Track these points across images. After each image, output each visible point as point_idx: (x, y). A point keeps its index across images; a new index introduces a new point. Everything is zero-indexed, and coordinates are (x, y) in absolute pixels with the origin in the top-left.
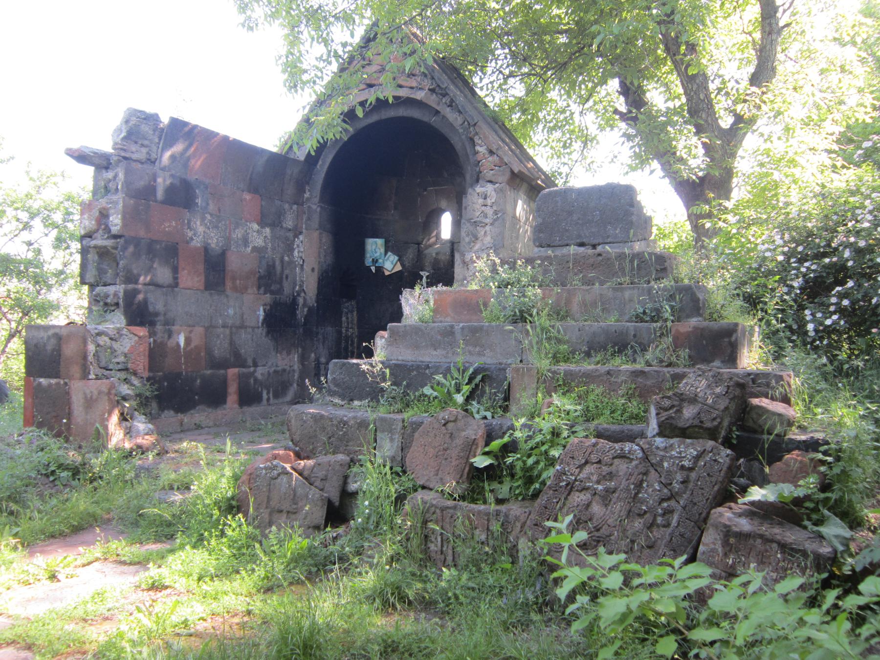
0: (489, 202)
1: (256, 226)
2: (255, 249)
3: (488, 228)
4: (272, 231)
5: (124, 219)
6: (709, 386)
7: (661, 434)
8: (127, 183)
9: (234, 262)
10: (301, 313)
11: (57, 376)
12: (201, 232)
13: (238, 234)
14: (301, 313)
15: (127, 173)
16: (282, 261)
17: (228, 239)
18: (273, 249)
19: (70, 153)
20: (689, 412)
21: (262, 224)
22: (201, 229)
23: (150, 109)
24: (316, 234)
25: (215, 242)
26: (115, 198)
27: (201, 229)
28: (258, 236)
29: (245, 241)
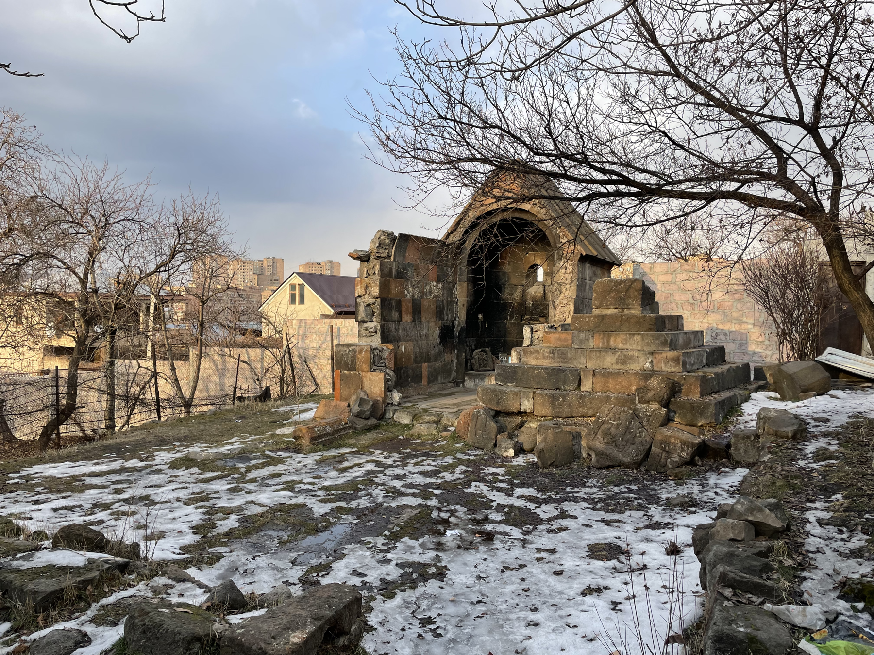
0: (568, 271)
1: (435, 283)
2: (435, 297)
3: (568, 286)
4: (443, 286)
5: (380, 289)
6: (658, 384)
7: (639, 402)
8: (381, 270)
9: (425, 303)
10: (457, 329)
11: (355, 369)
12: (411, 292)
13: (427, 289)
14: (457, 329)
15: (381, 265)
16: (447, 301)
17: (423, 292)
18: (443, 295)
19: (351, 255)
20: (650, 394)
21: (438, 282)
22: (411, 289)
23: (390, 231)
24: (465, 284)
25: (416, 295)
26: (374, 277)
27: (411, 289)
28: (435, 288)
29: (430, 292)
